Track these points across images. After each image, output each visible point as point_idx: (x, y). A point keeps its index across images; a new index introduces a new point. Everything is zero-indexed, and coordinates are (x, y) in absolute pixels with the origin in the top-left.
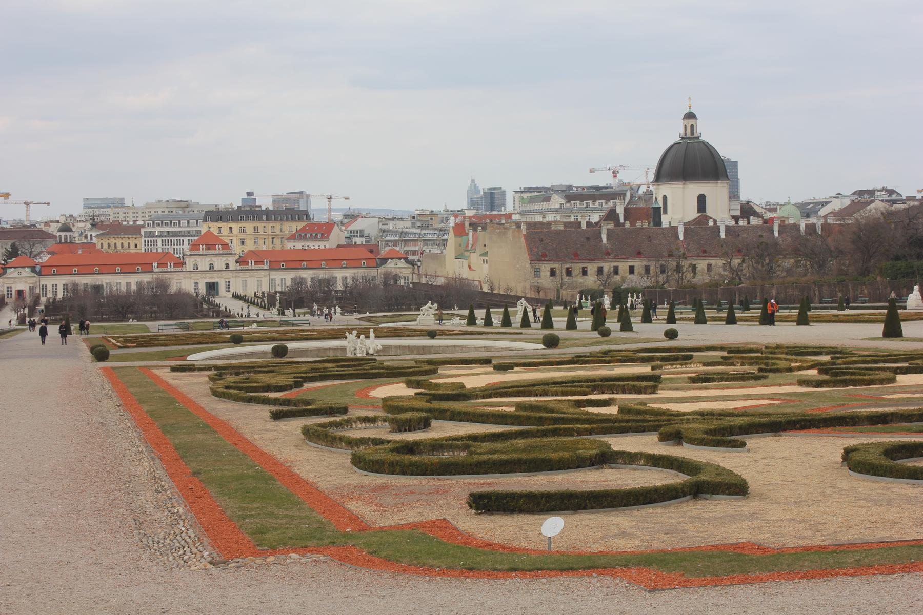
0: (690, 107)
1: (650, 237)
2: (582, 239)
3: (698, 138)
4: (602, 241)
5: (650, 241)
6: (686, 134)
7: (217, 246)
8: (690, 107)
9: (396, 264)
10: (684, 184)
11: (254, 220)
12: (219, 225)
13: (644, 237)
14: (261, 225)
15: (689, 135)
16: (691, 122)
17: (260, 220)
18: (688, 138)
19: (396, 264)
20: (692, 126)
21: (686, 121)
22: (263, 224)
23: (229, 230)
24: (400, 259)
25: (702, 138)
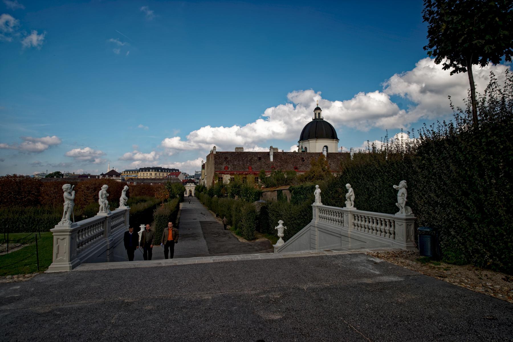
0: (317, 105)
1: (303, 158)
2: (256, 158)
3: (321, 119)
4: (270, 160)
5: (304, 161)
6: (316, 117)
7: (114, 176)
8: (317, 105)
9: (190, 185)
10: (316, 140)
11: (155, 171)
12: (144, 173)
13: (299, 158)
14: (158, 173)
15: (317, 117)
16: (318, 111)
17: (158, 171)
18: (317, 119)
19: (190, 185)
20: (319, 114)
21: (316, 112)
22: (159, 173)
23: (146, 175)
24: (192, 183)
25: (324, 120)
